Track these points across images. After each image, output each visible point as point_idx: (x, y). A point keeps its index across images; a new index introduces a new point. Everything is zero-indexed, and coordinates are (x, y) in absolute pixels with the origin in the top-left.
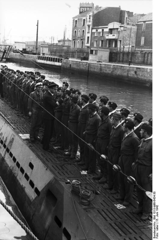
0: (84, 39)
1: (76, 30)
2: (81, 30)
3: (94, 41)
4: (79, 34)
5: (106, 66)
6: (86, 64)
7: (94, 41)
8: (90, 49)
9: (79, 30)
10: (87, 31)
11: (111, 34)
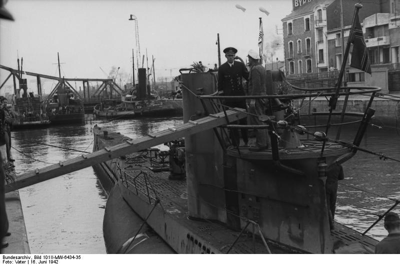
0: (313, 56)
1: (291, 41)
2: (303, 40)
3: (336, 55)
4: (299, 48)
5: (322, 103)
6: (358, 105)
7: (336, 55)
8: (348, 71)
9: (299, 39)
10: (317, 39)
11: (373, 37)
